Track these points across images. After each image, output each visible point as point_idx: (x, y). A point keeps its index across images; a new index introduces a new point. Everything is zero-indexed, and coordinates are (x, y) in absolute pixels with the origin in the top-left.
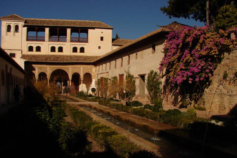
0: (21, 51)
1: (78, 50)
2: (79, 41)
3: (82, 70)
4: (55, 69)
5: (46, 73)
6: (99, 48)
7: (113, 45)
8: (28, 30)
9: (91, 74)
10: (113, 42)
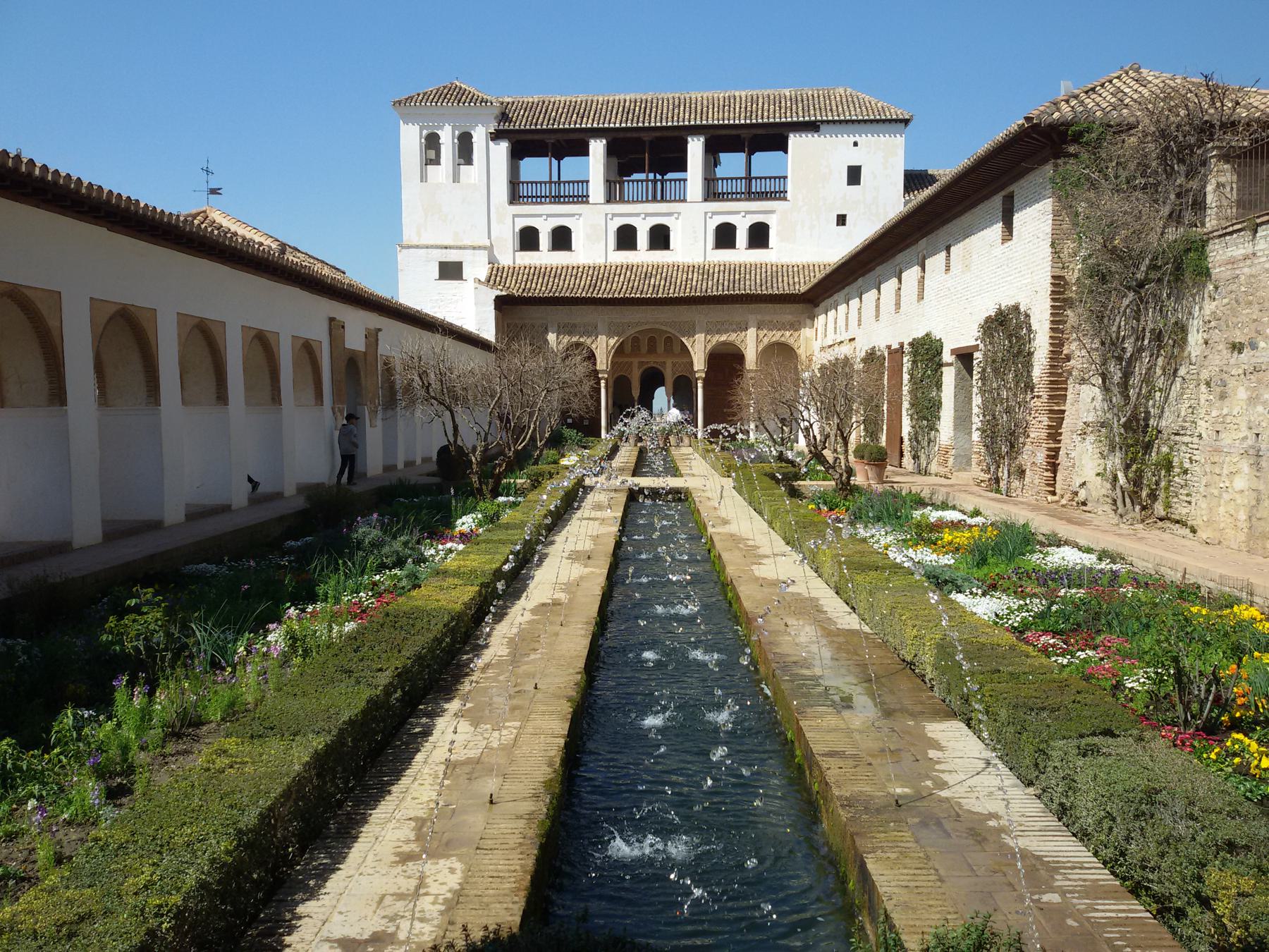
2: (751, 195)
4: (631, 331)
6: (842, 220)
8: (517, 154)
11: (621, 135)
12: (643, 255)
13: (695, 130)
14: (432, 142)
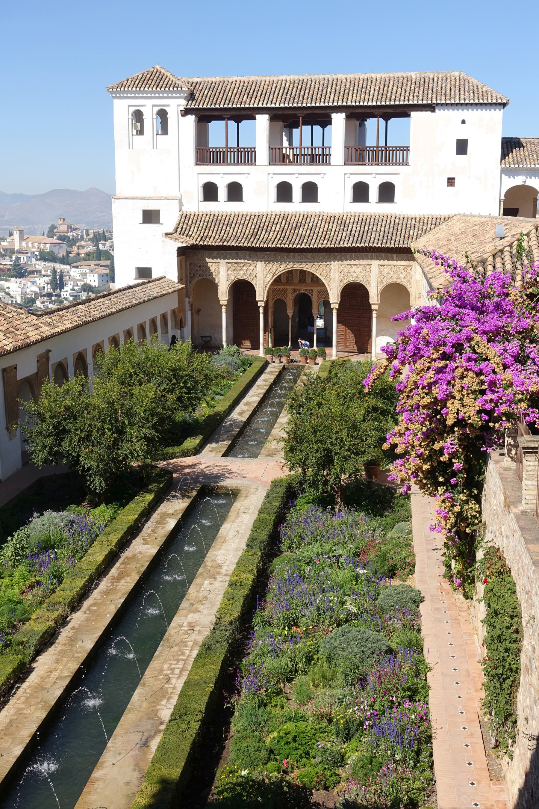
0: (177, 201)
1: (374, 193)
3: (374, 276)
5: (253, 283)
6: (451, 182)
7: (505, 171)
9: (408, 287)
10: (504, 155)
11: (281, 112)
12: (297, 206)
13: (338, 109)
14: (138, 116)
